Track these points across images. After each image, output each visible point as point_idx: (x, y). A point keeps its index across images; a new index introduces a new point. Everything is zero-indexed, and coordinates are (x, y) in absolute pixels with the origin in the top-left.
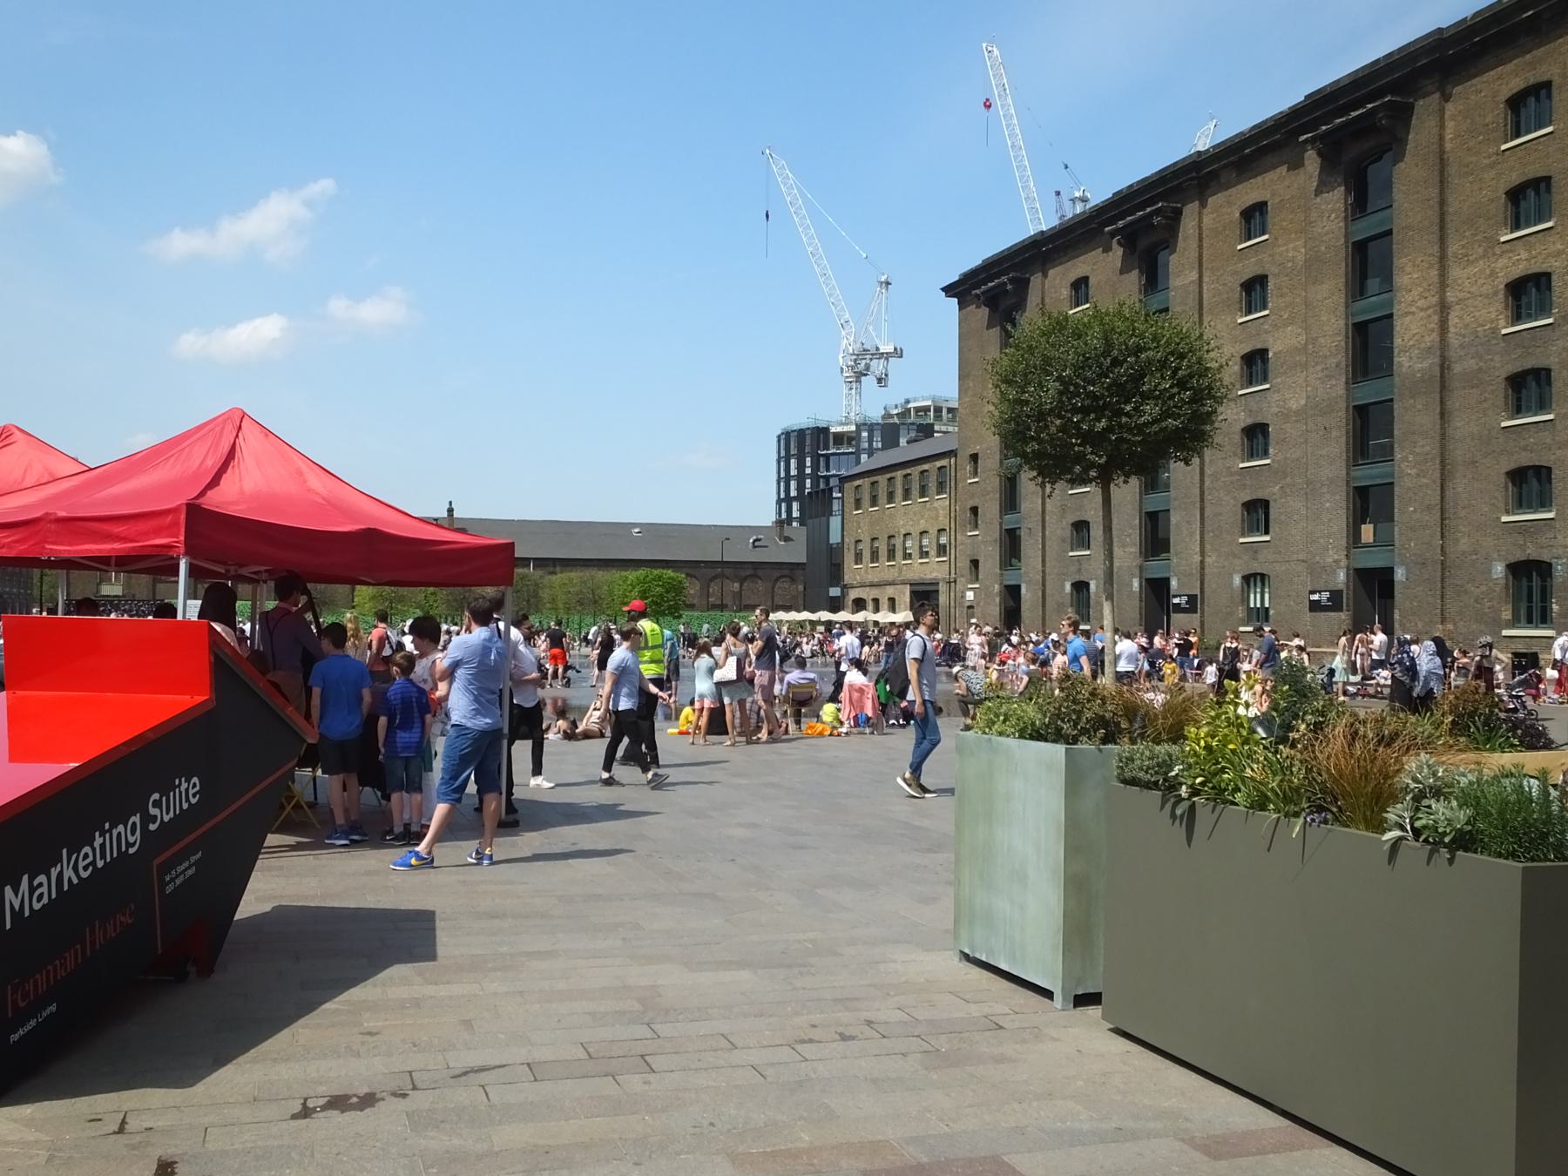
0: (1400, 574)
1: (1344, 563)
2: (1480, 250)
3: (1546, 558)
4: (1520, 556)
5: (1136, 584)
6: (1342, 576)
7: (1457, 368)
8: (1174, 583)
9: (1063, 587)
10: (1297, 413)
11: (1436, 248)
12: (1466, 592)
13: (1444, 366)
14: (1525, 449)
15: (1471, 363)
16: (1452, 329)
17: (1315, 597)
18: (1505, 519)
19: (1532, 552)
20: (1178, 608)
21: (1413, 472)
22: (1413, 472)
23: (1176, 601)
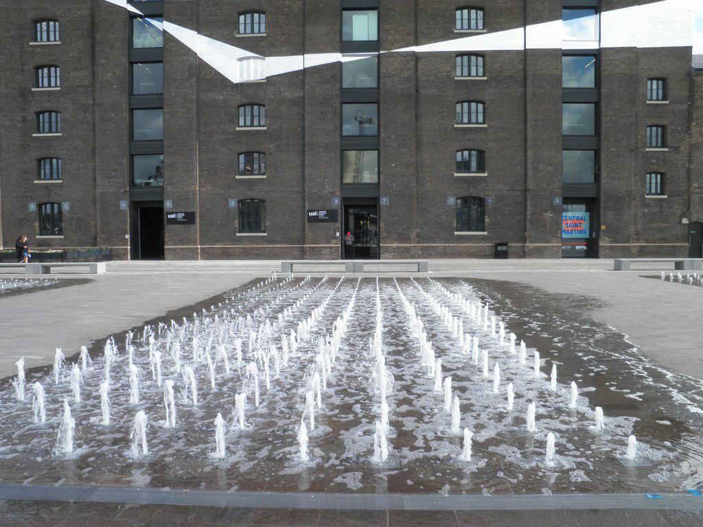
0: (384, 201)
1: (338, 193)
2: (440, 34)
3: (482, 195)
4: (465, 194)
5: (124, 205)
6: (336, 202)
7: (424, 92)
8: (168, 205)
9: (26, 207)
10: (291, 101)
11: (413, 25)
12: (429, 212)
13: (417, 91)
14: (469, 140)
15: (434, 91)
16: (420, 71)
17: (314, 214)
18: (456, 175)
19: (473, 192)
20: (174, 221)
21: (396, 144)
22: (396, 144)
23: (173, 216)
